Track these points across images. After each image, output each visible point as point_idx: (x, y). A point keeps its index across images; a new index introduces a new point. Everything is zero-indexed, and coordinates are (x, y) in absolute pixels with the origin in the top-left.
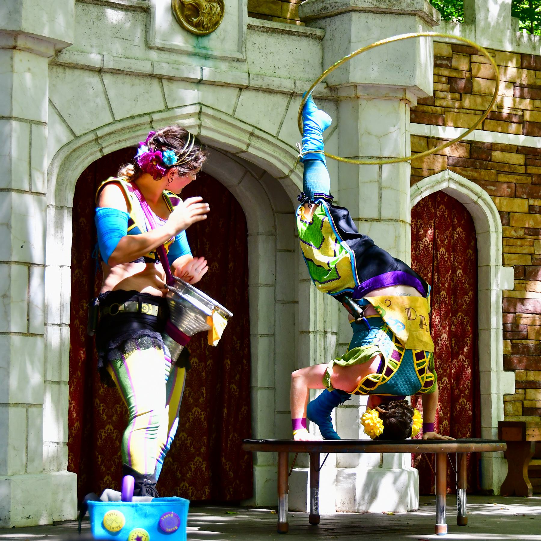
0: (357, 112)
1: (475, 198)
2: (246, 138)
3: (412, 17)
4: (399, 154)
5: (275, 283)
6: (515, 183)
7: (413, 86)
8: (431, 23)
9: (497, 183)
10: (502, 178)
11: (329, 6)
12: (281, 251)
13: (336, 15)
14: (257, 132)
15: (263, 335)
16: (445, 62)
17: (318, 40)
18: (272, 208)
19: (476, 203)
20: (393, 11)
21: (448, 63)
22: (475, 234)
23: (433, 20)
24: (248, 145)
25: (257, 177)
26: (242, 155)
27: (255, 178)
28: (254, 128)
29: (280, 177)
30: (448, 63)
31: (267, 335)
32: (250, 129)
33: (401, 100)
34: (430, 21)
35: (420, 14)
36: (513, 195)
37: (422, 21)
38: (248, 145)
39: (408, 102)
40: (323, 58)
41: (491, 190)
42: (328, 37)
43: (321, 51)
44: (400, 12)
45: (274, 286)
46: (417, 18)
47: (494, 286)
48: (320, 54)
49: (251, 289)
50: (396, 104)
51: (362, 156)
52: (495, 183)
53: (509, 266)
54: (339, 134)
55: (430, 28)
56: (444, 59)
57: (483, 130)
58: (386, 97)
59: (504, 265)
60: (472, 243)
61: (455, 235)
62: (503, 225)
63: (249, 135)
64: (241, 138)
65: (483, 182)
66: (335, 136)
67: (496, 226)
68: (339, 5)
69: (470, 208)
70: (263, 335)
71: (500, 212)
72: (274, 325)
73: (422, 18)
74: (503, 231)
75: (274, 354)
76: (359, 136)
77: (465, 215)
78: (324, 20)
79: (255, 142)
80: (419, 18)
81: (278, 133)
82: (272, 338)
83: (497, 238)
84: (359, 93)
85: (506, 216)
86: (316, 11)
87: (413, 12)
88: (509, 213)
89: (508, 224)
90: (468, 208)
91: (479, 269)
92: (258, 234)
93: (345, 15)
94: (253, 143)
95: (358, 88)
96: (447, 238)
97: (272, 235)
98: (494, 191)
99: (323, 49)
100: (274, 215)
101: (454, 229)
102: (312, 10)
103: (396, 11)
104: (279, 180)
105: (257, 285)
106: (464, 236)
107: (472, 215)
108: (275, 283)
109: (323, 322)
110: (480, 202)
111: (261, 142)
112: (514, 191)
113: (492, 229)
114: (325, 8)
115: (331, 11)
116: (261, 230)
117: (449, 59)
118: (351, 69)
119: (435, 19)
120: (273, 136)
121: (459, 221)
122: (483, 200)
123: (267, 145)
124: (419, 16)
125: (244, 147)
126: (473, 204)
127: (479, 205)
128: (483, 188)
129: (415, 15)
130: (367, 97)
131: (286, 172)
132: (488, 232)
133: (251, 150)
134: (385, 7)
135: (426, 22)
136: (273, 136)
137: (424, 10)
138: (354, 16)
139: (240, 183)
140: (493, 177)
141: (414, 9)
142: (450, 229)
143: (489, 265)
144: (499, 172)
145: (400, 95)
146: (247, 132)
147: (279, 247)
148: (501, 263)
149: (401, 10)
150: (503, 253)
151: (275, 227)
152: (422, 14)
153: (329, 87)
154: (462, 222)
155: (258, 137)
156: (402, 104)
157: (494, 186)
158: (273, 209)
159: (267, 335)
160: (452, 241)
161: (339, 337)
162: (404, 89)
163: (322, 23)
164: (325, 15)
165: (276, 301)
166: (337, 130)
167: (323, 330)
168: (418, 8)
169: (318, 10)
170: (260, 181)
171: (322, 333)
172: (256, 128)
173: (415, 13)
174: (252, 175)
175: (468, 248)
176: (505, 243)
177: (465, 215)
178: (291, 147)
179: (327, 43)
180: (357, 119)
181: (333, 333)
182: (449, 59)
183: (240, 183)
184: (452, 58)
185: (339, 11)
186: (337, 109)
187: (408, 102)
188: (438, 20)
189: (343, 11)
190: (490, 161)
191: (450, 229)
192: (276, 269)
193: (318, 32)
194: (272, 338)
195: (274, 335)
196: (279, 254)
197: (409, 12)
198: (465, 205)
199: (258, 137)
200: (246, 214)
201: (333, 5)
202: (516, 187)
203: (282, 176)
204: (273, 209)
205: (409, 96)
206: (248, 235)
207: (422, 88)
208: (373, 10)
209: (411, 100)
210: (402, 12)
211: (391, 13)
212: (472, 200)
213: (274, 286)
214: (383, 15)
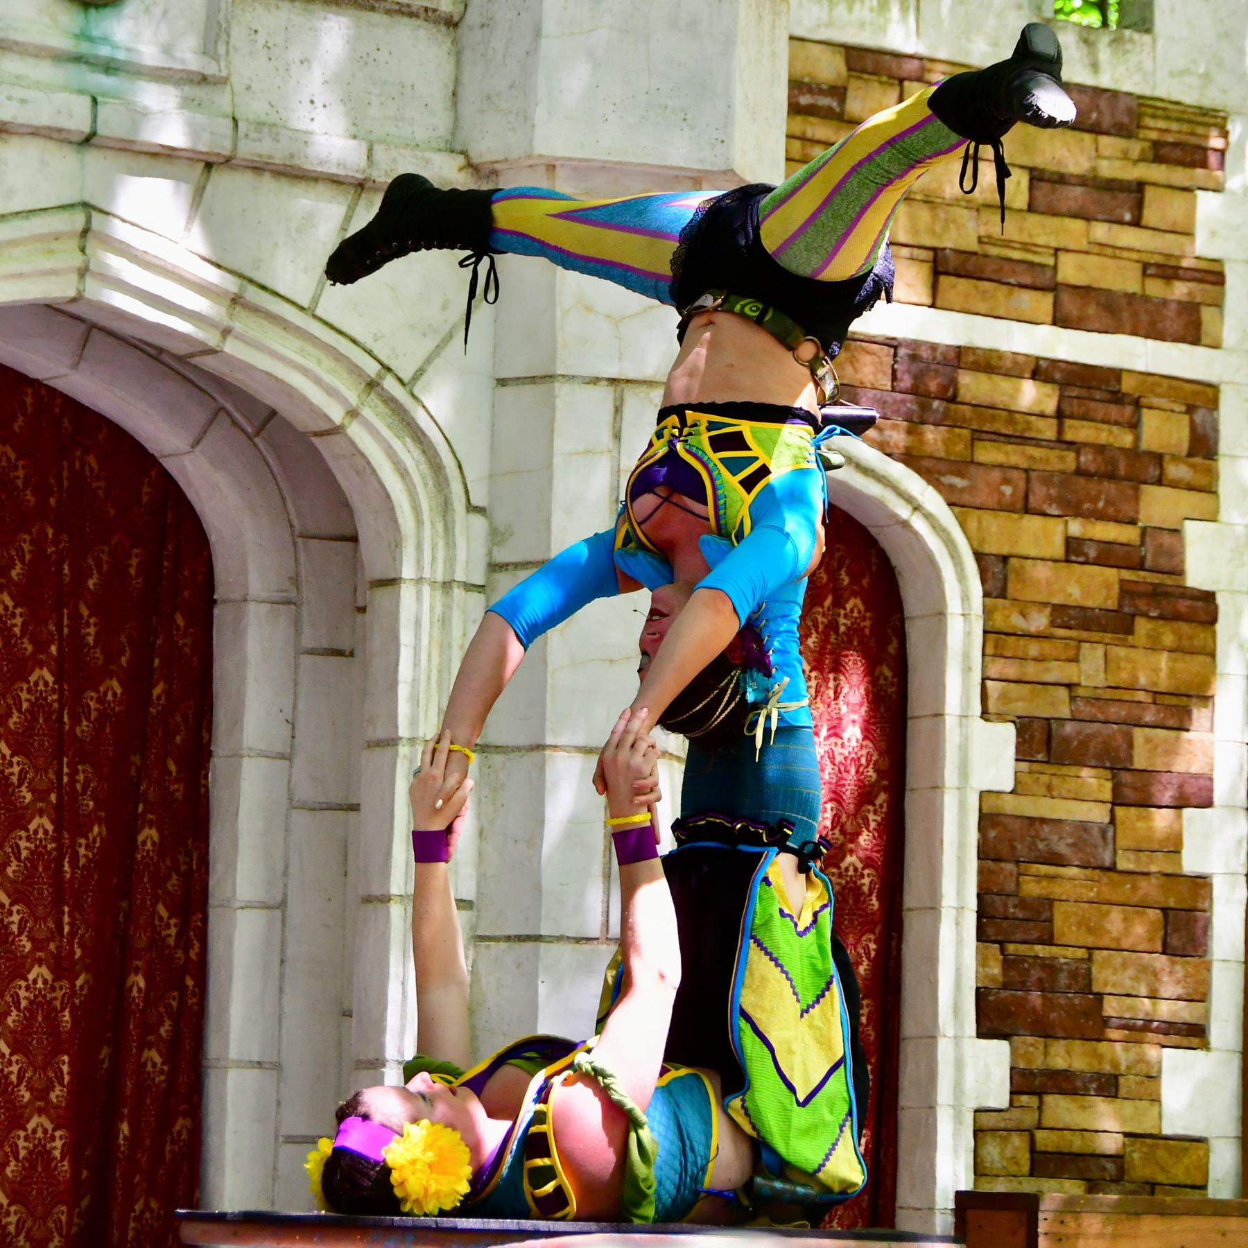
1: (903, 511)
6: (1026, 471)
9: (973, 470)
10: (988, 453)
16: (824, 101)
19: (905, 524)
21: (835, 104)
22: (902, 620)
30: (835, 104)
36: (1020, 505)
41: (952, 487)
47: (950, 776)
52: (963, 466)
53: (1001, 718)
56: (821, 92)
57: (933, 306)
59: (985, 715)
60: (892, 648)
61: (842, 620)
62: (986, 595)
65: (926, 463)
67: (965, 598)
69: (888, 540)
71: (979, 556)
74: (987, 613)
77: (874, 560)
85: (997, 569)
88: (1005, 559)
89: (1003, 595)
90: (884, 542)
91: (910, 723)
96: (816, 627)
98: (963, 490)
101: (839, 603)
106: (867, 623)
110: (919, 524)
112: (1021, 494)
113: (953, 605)
117: (839, 92)
121: (855, 579)
122: (928, 517)
128: (929, 482)
132: (941, 615)
140: (960, 447)
142: (828, 602)
143: (939, 715)
144: (978, 436)
148: (977, 708)
150: (983, 680)
154: (865, 582)
157: (960, 474)
160: (833, 638)
175: (880, 662)
176: (989, 651)
177: (874, 560)
182: (839, 92)
184: (845, 89)
190: (953, 400)
191: (828, 602)
198: (873, 531)
202: (1028, 481)
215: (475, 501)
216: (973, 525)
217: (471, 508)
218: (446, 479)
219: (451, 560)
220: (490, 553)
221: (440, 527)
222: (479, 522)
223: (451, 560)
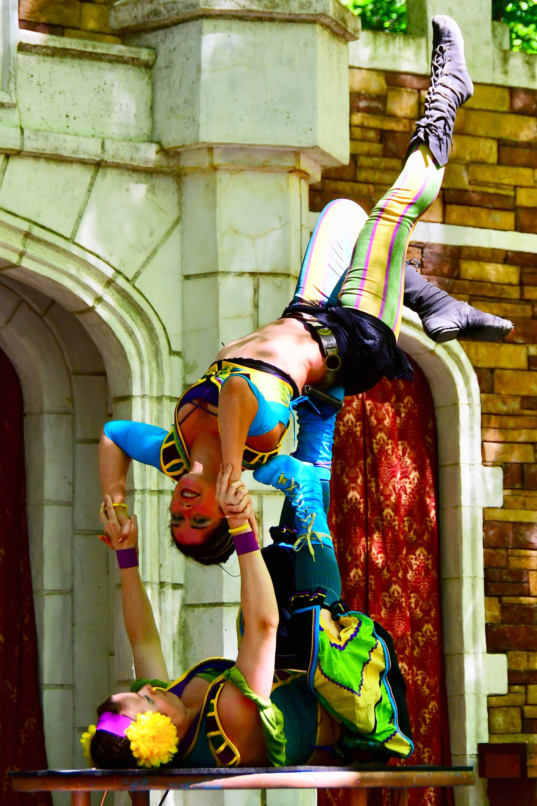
0: (214, 192)
2: (17, 242)
3: (308, 28)
4: (288, 268)
5: (73, 498)
7: (313, 148)
8: (343, 36)
11: (162, 8)
12: (83, 441)
13: (176, 24)
14: (37, 232)
15: (52, 592)
17: (143, 70)
18: (66, 365)
19: (432, 352)
20: (275, 16)
23: (347, 31)
24: (22, 255)
25: (40, 312)
26: (12, 272)
27: (36, 313)
28: (32, 225)
29: (78, 310)
31: (60, 592)
32: (25, 226)
33: (291, 172)
34: (342, 32)
35: (323, 20)
37: (326, 33)
38: (22, 255)
39: (304, 175)
40: (153, 101)
42: (161, 62)
43: (149, 87)
44: (287, 17)
45: (70, 504)
46: (318, 28)
48: (148, 93)
49: (30, 509)
50: (282, 178)
51: (223, 272)
54: (182, 233)
55: (341, 44)
58: (264, 168)
62: (482, 392)
63: (21, 237)
64: (9, 243)
66: (176, 235)
68: (181, 6)
69: (423, 361)
70: (52, 592)
71: (477, 369)
72: (73, 573)
73: (326, 27)
74: (483, 403)
75: (73, 625)
76: (218, 234)
78: (155, 34)
79: (33, 249)
80: (321, 28)
81: (74, 233)
82: (69, 597)
83: (472, 415)
84: (218, 160)
85: (488, 376)
86: (139, 17)
87: (310, 18)
92: (41, 412)
93: (190, 24)
94: (29, 251)
95: (216, 152)
97: (67, 413)
99: (153, 85)
100: (70, 378)
102: (133, 15)
103: (280, 16)
104: (78, 317)
105: (41, 504)
107: (428, 374)
108: (73, 498)
109: (157, 566)
111: (45, 248)
114: (156, 13)
115: (165, 16)
116: (47, 403)
118: (202, 118)
119: (349, 30)
120: (66, 239)
123: (57, 254)
124: (322, 25)
125: (14, 258)
126: (428, 355)
127: (438, 357)
129: (314, 22)
130: (232, 167)
131: (90, 302)
132: (456, 405)
133: (26, 264)
134: (261, 9)
135: (334, 34)
136: (66, 239)
137: (331, 13)
138: (207, 24)
139: (8, 321)
141: (312, 11)
145: (290, 162)
146: (20, 231)
147: (80, 435)
149: (290, 14)
151: (71, 400)
152: (327, 21)
153: (163, 151)
155: (39, 240)
156: (294, 179)
158: (68, 368)
159: (60, 592)
161: (186, 593)
162: (297, 153)
163: (151, 38)
164: (157, 25)
165: (75, 532)
166: (179, 226)
167: (157, 580)
168: (319, 10)
169: (143, 16)
170: (45, 318)
171: (156, 587)
172: (35, 224)
173: (314, 18)
174: (31, 308)
178: (98, 257)
179: (161, 74)
180: (213, 206)
181: (176, 586)
183: (8, 321)
185: (180, 17)
186: (179, 189)
187: (304, 175)
188: (356, 31)
189: (188, 17)
192: (74, 474)
193: (144, 55)
194: (69, 597)
195: (72, 591)
196: (80, 447)
197: (303, 17)
199: (39, 240)
200: (21, 377)
201: (170, 6)
203: (83, 308)
204: (68, 368)
205: (305, 164)
206: (23, 415)
207: (327, 150)
208: (239, 14)
209: (310, 172)
210: (292, 17)
211: (272, 20)
212: (425, 348)
213: (70, 504)
214: (258, 23)
215: (174, 348)
216: (473, 351)
217: (172, 353)
218: (156, 336)
219: (161, 384)
220: (184, 379)
221: (154, 364)
222: (177, 361)
223: (161, 384)
